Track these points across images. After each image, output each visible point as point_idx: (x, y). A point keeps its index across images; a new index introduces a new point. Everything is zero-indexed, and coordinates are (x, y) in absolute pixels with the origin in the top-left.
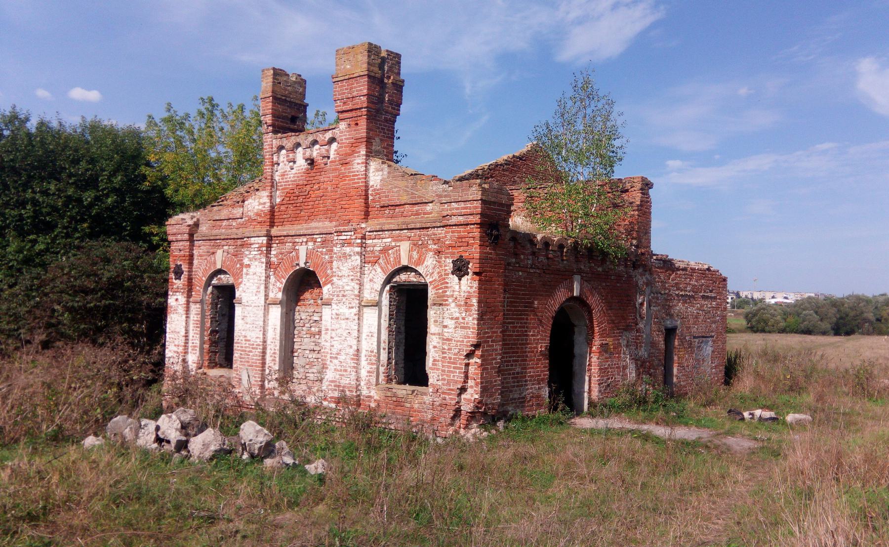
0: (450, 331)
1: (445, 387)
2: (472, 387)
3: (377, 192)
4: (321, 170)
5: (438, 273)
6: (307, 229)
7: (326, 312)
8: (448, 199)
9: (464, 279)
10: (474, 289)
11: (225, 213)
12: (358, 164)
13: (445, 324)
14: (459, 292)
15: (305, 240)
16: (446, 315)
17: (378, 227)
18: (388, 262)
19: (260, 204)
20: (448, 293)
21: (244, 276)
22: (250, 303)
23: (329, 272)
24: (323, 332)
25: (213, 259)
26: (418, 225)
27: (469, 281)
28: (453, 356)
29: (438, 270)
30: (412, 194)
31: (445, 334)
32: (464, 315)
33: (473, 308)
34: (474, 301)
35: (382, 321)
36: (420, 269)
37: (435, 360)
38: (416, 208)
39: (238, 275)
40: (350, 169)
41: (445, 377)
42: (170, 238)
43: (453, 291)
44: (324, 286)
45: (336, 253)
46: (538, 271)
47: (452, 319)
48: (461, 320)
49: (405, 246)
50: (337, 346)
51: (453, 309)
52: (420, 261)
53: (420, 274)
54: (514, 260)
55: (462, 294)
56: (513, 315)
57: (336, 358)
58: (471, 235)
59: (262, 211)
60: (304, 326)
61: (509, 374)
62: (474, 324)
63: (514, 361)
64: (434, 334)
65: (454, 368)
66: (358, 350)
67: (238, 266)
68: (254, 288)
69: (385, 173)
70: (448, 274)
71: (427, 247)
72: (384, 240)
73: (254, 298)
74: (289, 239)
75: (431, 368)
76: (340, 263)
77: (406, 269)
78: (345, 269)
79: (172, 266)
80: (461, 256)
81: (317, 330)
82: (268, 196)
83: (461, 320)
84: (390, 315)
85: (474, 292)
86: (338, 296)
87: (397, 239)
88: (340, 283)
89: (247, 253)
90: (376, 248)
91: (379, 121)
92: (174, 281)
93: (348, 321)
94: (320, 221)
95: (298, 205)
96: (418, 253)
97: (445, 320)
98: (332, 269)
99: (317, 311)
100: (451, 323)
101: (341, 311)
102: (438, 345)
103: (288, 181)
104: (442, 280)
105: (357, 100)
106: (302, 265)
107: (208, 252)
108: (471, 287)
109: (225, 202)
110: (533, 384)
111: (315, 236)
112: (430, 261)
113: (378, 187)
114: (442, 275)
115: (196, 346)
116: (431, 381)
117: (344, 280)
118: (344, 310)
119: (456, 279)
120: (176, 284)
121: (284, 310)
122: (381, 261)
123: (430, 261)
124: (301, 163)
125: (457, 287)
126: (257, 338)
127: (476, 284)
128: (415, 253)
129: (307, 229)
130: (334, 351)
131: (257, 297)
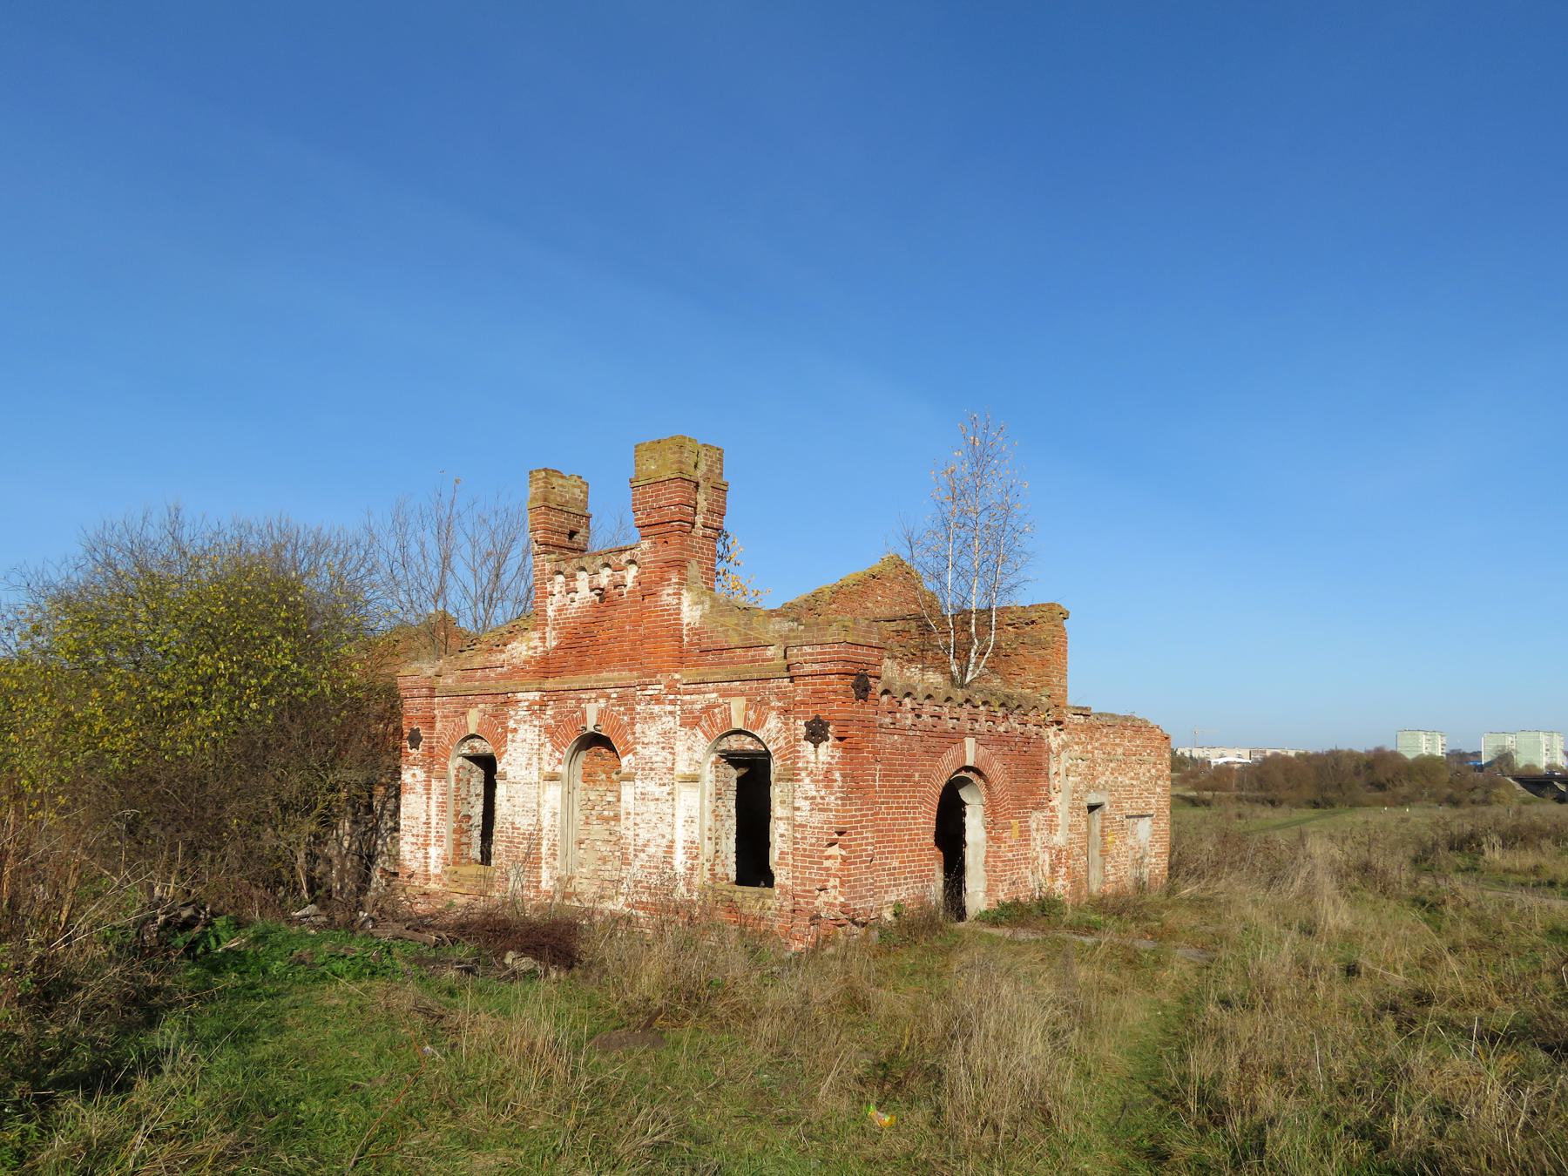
0: (803, 814)
1: (799, 888)
2: (835, 887)
3: (695, 632)
4: (613, 604)
5: (785, 738)
6: (597, 681)
7: (627, 791)
8: (798, 642)
9: (823, 746)
10: (836, 760)
11: (478, 661)
12: (668, 595)
13: (796, 805)
14: (816, 763)
15: (594, 695)
16: (798, 794)
17: (698, 679)
18: (713, 724)
19: (529, 648)
20: (800, 765)
21: (509, 743)
22: (518, 779)
23: (630, 738)
24: (623, 817)
25: (463, 721)
26: (756, 676)
27: (830, 749)
28: (808, 848)
29: (784, 734)
30: (746, 634)
31: (797, 818)
32: (822, 793)
33: (835, 784)
34: (837, 775)
35: (706, 802)
36: (759, 734)
37: (782, 853)
38: (751, 653)
39: (501, 741)
40: (657, 601)
41: (797, 874)
42: (403, 694)
43: (807, 762)
44: (623, 757)
45: (639, 713)
46: (918, 733)
47: (806, 798)
48: (819, 800)
49: (737, 706)
50: (644, 835)
51: (808, 786)
52: (760, 723)
53: (758, 740)
55: (820, 766)
56: (887, 792)
57: (644, 851)
58: (831, 688)
59: (532, 657)
60: (593, 809)
61: (884, 870)
62: (838, 805)
63: (889, 852)
64: (781, 819)
65: (810, 862)
67: (500, 730)
68: (523, 760)
69: (707, 606)
70: (799, 740)
71: (768, 704)
72: (707, 696)
73: (524, 772)
74: (572, 694)
75: (777, 864)
76: (646, 726)
77: (739, 732)
78: (652, 734)
79: (407, 731)
80: (817, 716)
81: (612, 814)
82: (540, 638)
83: (819, 800)
84: (717, 794)
85: (837, 763)
86: (643, 769)
87: (725, 694)
88: (646, 752)
89: (512, 713)
90: (696, 706)
91: (695, 537)
92: (409, 750)
93: (659, 802)
94: (613, 671)
95: (584, 649)
96: (755, 712)
97: (796, 801)
98: (634, 733)
99: (610, 788)
100: (805, 805)
101: (648, 789)
102: (786, 833)
103: (568, 618)
104: (792, 750)
105: (666, 511)
106: (591, 729)
107: (456, 712)
108: (833, 757)
109: (478, 646)
110: (915, 882)
111: (608, 691)
112: (773, 723)
113: (697, 625)
114: (790, 742)
115: (442, 837)
116: (777, 880)
117: (652, 749)
118: (652, 788)
119: (811, 746)
120: (412, 754)
122: (703, 723)
123: (773, 723)
124: (584, 593)
125: (812, 758)
126: (530, 825)
127: (838, 754)
128: (751, 712)
129: (597, 681)
130: (640, 842)
131: (528, 772)
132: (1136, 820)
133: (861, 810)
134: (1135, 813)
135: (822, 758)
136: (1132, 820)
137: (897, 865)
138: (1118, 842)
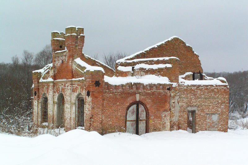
54: (108, 91)
66: (71, 117)
119: (87, 96)
121: (58, 106)
124: (61, 61)
132: (211, 115)
133: (98, 111)
134: (210, 113)
135: (89, 100)
136: (209, 115)
137: (111, 123)
138: (202, 121)
